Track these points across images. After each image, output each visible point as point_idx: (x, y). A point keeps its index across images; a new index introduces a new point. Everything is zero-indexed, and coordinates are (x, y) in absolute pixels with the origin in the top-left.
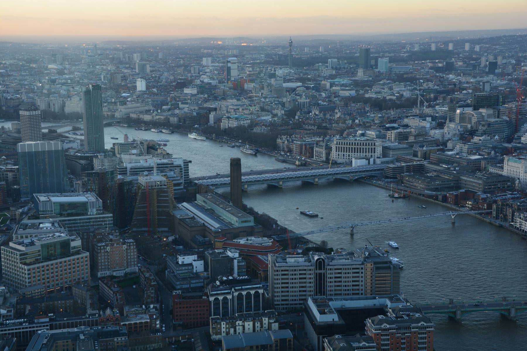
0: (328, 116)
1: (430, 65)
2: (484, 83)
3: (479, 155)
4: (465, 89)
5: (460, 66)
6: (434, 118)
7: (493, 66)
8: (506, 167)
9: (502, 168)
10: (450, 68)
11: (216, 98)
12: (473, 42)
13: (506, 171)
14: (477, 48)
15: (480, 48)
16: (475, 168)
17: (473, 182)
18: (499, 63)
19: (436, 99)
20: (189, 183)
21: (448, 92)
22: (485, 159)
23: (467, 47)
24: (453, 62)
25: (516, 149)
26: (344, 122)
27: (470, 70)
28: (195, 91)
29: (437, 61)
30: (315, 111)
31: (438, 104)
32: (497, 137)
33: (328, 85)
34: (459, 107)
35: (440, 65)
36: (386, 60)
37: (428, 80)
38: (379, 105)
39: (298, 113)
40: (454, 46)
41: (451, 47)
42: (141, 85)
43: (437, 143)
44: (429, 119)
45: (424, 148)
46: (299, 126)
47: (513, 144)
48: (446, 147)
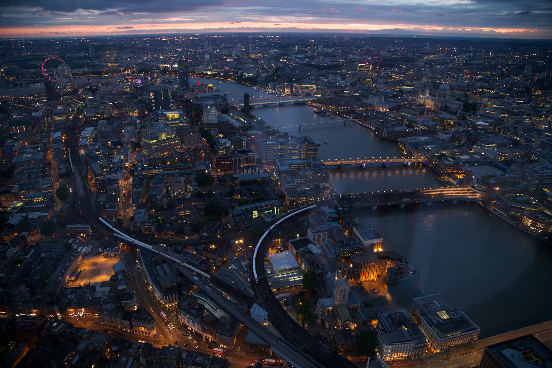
0: (293, 73)
6: (341, 75)
9: (368, 100)
11: (241, 63)
12: (362, 39)
14: (363, 42)
16: (357, 99)
20: (227, 104)
23: (359, 41)
26: (300, 76)
28: (232, 60)
30: (287, 70)
33: (294, 58)
36: (322, 46)
38: (318, 67)
39: (279, 71)
41: (352, 41)
42: (207, 57)
43: (341, 87)
44: (338, 75)
46: (279, 77)
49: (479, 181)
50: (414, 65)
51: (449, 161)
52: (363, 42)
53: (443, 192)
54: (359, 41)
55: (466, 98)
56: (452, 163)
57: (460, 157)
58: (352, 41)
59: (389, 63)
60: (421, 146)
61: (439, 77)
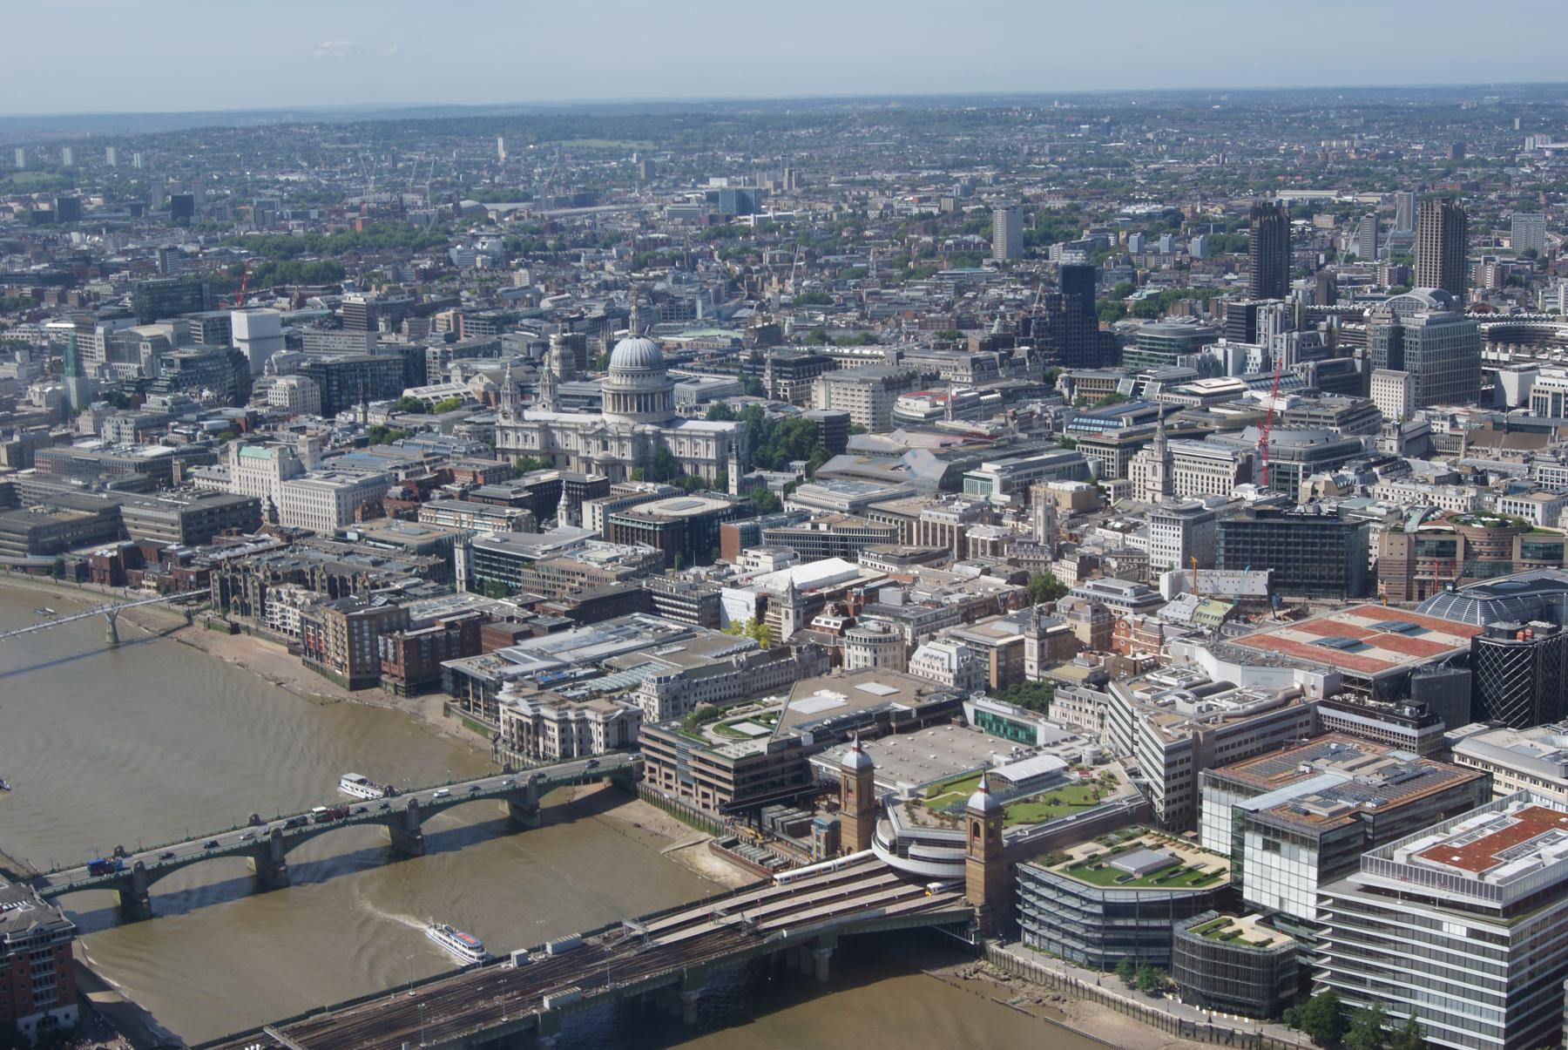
1: (16, 207)
2: (163, 252)
3: (166, 444)
4: (117, 268)
5: (99, 207)
7: (182, 209)
8: (235, 472)
10: (70, 212)
12: (125, 144)
13: (236, 480)
14: (137, 160)
15: (147, 158)
16: (157, 476)
17: (154, 519)
18: (199, 199)
19: (39, 296)
21: (69, 280)
22: (182, 453)
24: (77, 200)
25: (254, 421)
27: (127, 219)
29: (35, 196)
31: (46, 315)
32: (206, 393)
34: (103, 318)
35: (44, 207)
37: (14, 249)
40: (76, 156)
45: (16, 439)
47: (249, 408)
48: (77, 429)
49: (921, 813)
50: (450, 262)
51: (745, 737)
52: (137, 160)
53: (750, 914)
54: (111, 153)
55: (753, 401)
56: (762, 746)
57: (793, 706)
58: (67, 157)
59: (310, 260)
60: (576, 681)
61: (598, 311)
